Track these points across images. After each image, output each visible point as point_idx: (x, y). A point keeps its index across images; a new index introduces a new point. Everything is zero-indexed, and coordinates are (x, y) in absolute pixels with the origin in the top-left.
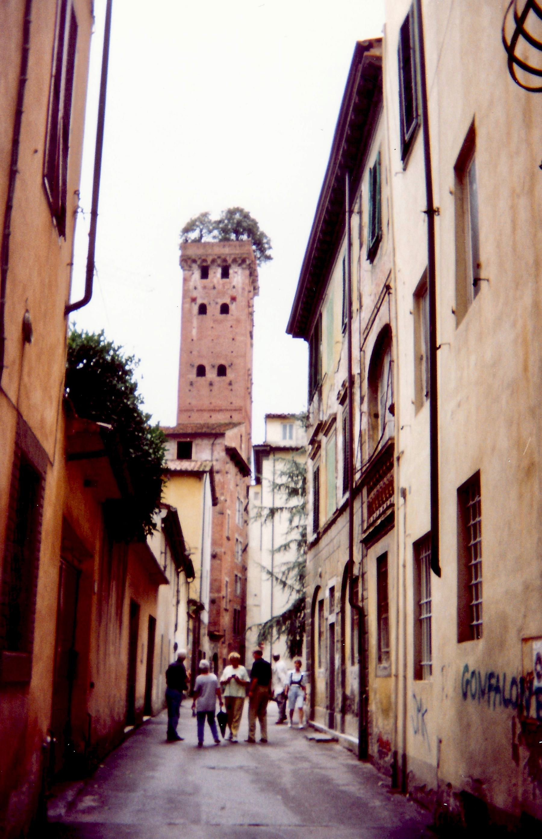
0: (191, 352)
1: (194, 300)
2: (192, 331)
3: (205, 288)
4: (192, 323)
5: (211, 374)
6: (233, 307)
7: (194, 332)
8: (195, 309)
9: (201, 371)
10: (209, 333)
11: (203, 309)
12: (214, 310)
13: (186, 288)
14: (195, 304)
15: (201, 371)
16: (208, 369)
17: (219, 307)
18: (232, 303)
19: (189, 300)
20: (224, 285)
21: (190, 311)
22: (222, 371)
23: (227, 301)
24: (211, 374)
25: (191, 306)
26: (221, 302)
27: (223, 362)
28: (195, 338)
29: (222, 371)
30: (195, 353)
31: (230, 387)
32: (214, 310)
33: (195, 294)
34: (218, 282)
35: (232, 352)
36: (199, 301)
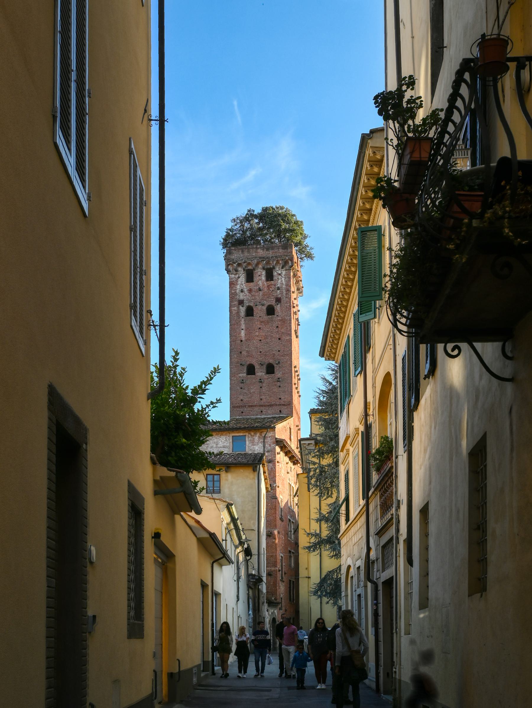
0: (241, 352)
1: (241, 302)
2: (240, 333)
3: (250, 291)
4: (240, 325)
5: (260, 373)
6: (278, 308)
7: (243, 333)
8: (243, 310)
9: (251, 370)
10: (257, 334)
11: (250, 312)
12: (260, 311)
13: (233, 292)
14: (242, 306)
15: (251, 370)
16: (257, 367)
17: (265, 308)
18: (278, 304)
19: (236, 303)
20: (269, 287)
21: (238, 312)
22: (270, 369)
23: (273, 303)
24: (260, 373)
25: (238, 308)
26: (267, 304)
27: (271, 361)
28: (243, 339)
29: (270, 369)
30: (244, 353)
31: (279, 384)
32: (260, 311)
33: (242, 296)
34: (263, 285)
35: (279, 351)
36: (246, 304)
